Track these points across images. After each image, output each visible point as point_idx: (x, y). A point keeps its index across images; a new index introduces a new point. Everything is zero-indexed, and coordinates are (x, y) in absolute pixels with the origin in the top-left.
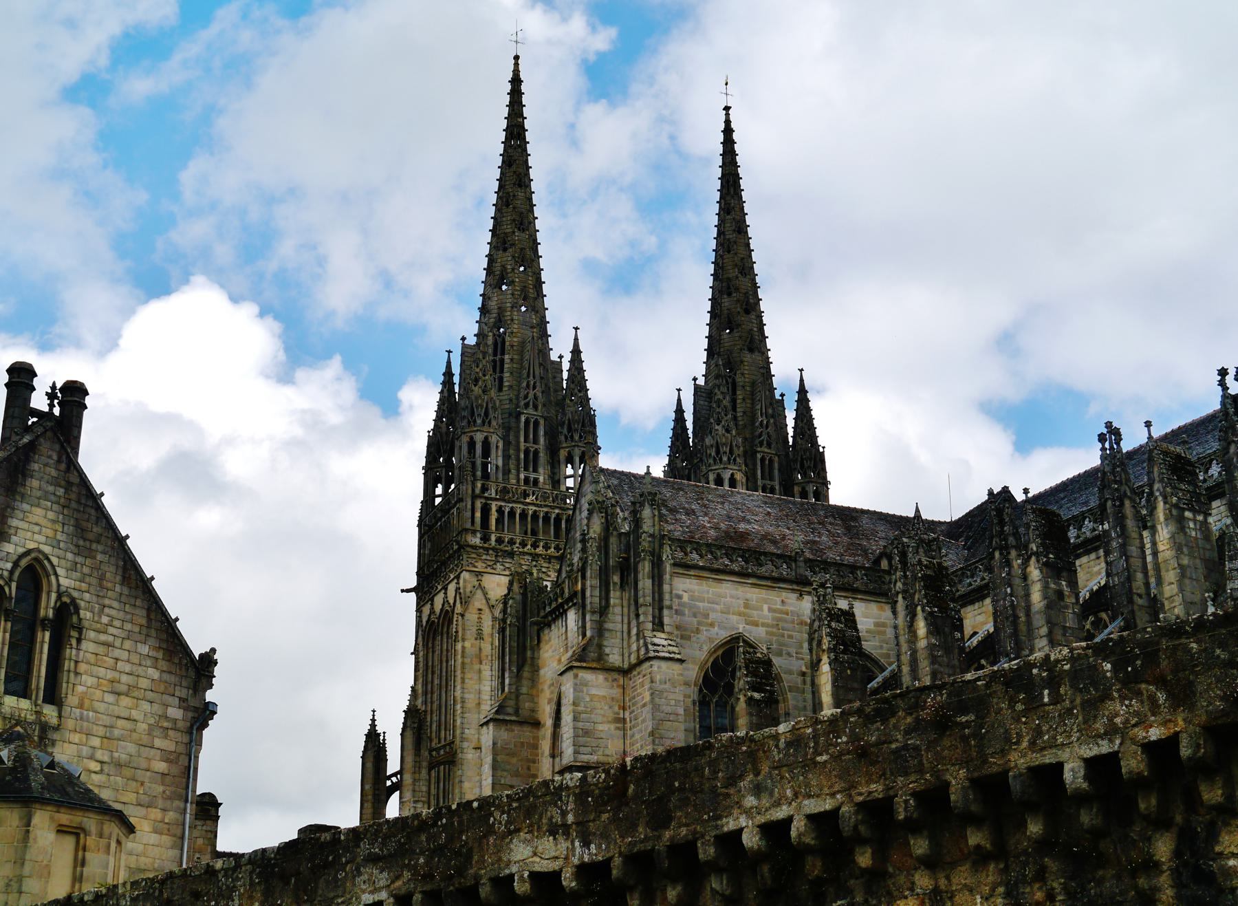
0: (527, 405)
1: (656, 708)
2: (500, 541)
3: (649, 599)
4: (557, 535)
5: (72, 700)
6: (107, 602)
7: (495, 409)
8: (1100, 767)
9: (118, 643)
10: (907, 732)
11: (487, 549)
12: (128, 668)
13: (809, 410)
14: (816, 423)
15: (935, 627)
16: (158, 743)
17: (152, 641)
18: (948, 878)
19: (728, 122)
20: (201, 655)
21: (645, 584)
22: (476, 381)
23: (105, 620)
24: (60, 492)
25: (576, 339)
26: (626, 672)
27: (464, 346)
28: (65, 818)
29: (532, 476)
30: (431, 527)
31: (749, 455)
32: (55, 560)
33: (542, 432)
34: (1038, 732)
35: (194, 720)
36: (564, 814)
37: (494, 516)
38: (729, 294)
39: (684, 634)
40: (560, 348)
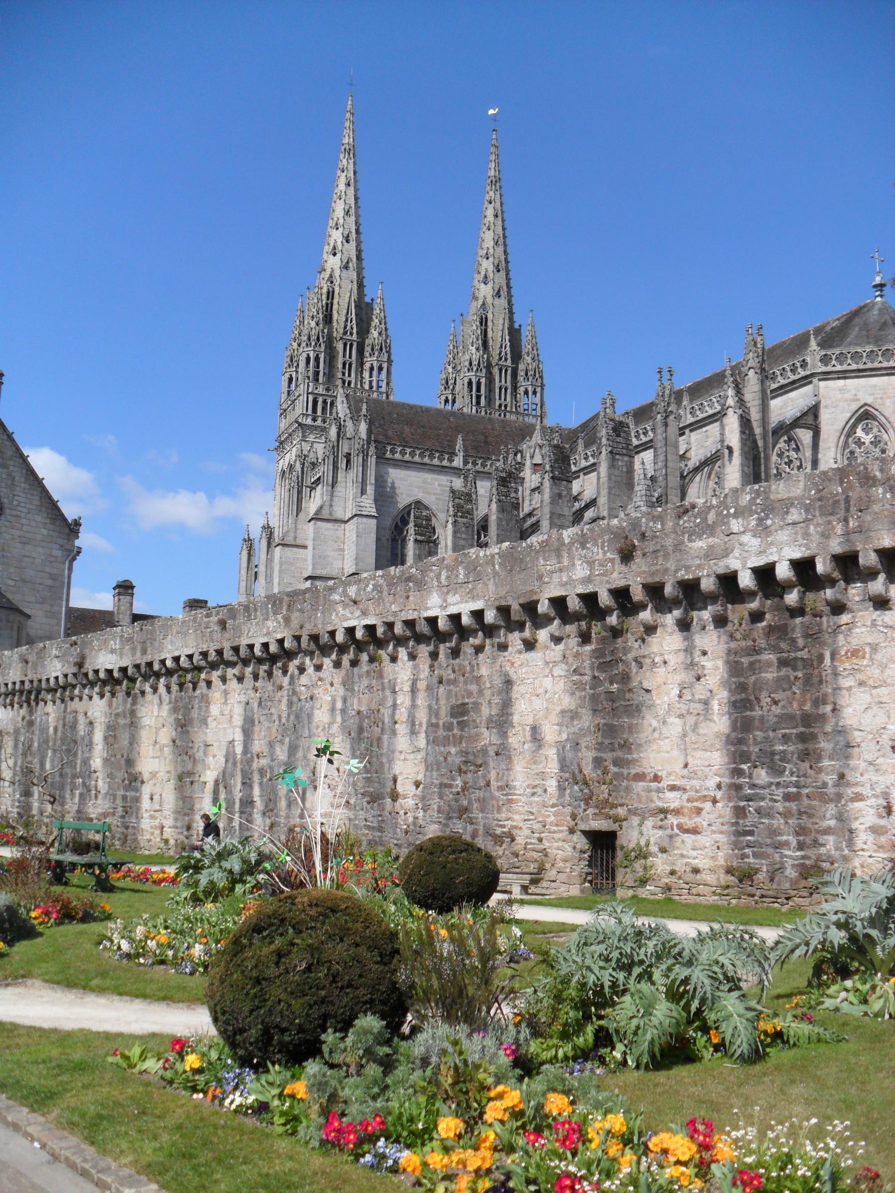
9: (23, 515)
16: (47, 569)
17: (45, 515)
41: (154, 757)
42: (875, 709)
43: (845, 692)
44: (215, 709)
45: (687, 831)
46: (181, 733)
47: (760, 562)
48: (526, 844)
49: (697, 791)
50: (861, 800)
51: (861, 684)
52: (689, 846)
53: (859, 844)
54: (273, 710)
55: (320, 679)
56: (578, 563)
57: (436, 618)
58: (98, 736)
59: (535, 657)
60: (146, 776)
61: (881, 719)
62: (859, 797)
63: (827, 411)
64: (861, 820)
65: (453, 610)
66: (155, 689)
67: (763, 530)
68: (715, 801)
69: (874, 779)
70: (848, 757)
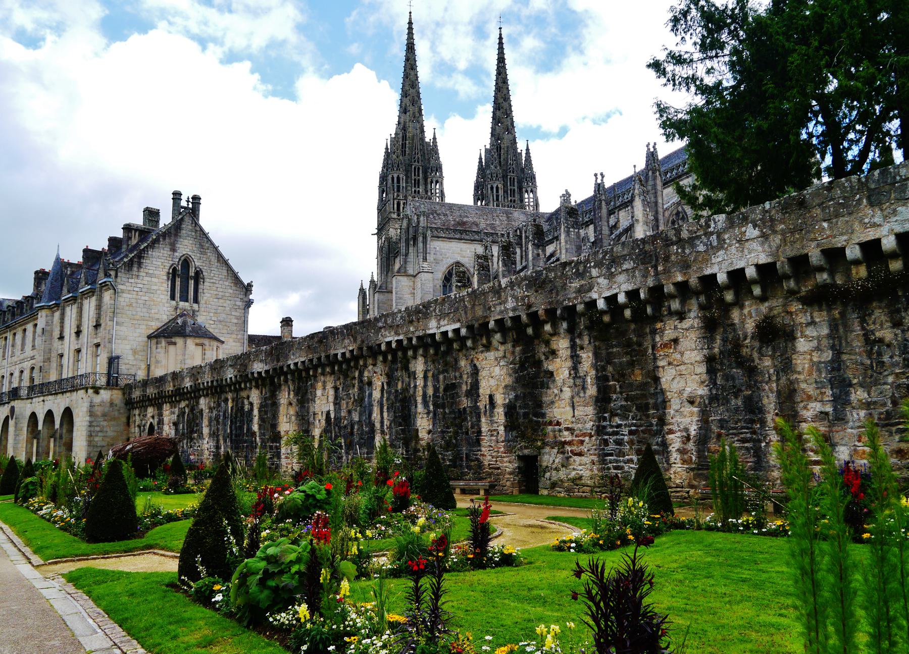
0: (415, 161)
1: (422, 289)
3: (422, 250)
7: (401, 163)
9: (217, 282)
12: (221, 290)
13: (530, 157)
14: (533, 162)
16: (233, 313)
17: (229, 281)
19: (500, 35)
21: (421, 245)
23: (212, 275)
24: (193, 234)
26: (415, 276)
28: (198, 341)
29: (417, 189)
30: (381, 210)
31: (505, 177)
33: (421, 172)
35: (246, 305)
38: (499, 110)
39: (437, 262)
40: (428, 137)
42: (678, 378)
43: (661, 369)
44: (319, 393)
45: (576, 454)
47: (607, 294)
48: (489, 465)
49: (581, 431)
50: (673, 433)
51: (670, 364)
52: (577, 463)
53: (672, 460)
54: (350, 392)
55: (375, 372)
56: (510, 299)
57: (435, 334)
58: (256, 412)
59: (491, 355)
61: (682, 384)
62: (671, 432)
64: (673, 446)
65: (443, 329)
66: (286, 381)
67: (611, 276)
68: (591, 436)
69: (679, 420)
70: (665, 408)
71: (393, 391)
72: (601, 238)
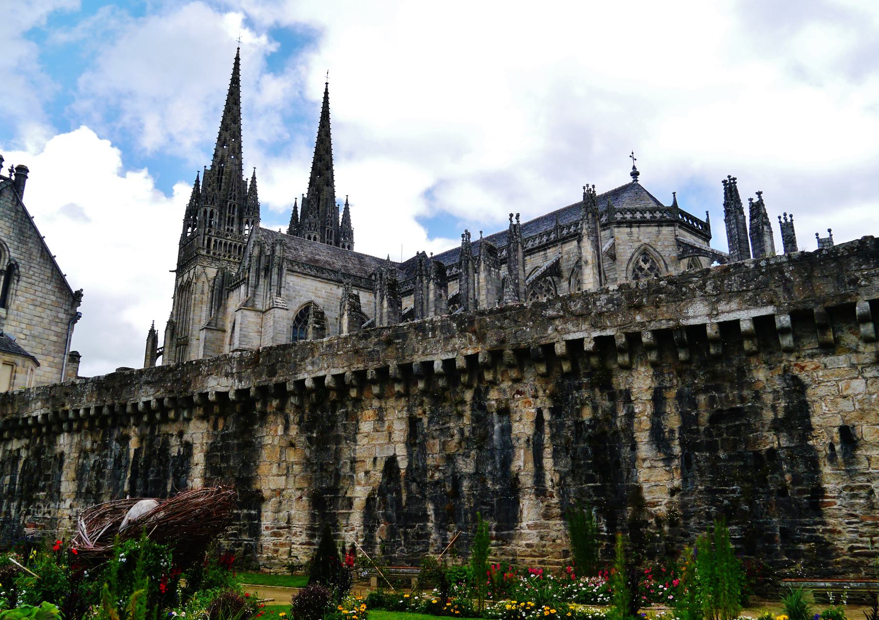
0: (231, 198)
1: (275, 328)
2: (214, 254)
3: (276, 283)
4: (239, 254)
5: (13, 307)
6: (32, 265)
7: (217, 198)
8: (449, 364)
9: (37, 283)
10: (375, 344)
11: (209, 257)
12: (41, 295)
13: (349, 212)
15: (391, 304)
16: (53, 328)
17: (53, 284)
18: (385, 403)
19: (327, 89)
20: (76, 292)
21: (275, 277)
22: (209, 186)
23: (31, 273)
24: (13, 214)
25: (254, 173)
26: (263, 312)
27: (205, 170)
28: (7, 358)
29: (231, 228)
30: (185, 245)
31: (323, 228)
32: (8, 245)
33: (236, 210)
34: (426, 348)
35: (71, 320)
36: (232, 369)
37: (213, 243)
38: (321, 161)
39: (289, 299)
40: (247, 175)
41: (278, 475)
44: (366, 426)
46: (317, 451)
57: (703, 326)
58: (199, 457)
60: (266, 494)
63: (620, 247)
66: (281, 409)
71: (569, 423)
72: (518, 283)
